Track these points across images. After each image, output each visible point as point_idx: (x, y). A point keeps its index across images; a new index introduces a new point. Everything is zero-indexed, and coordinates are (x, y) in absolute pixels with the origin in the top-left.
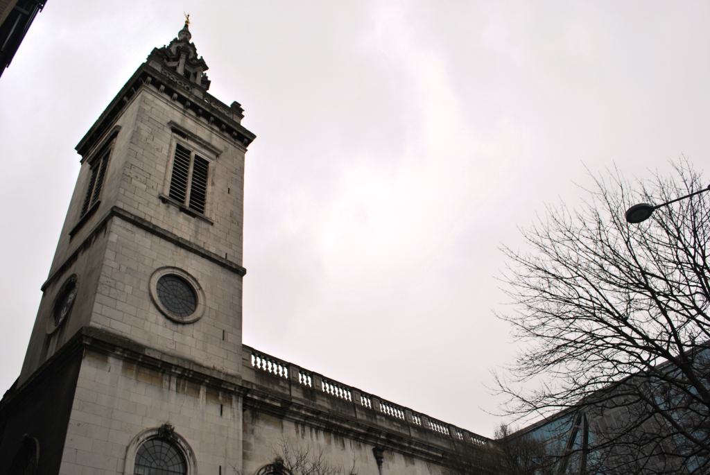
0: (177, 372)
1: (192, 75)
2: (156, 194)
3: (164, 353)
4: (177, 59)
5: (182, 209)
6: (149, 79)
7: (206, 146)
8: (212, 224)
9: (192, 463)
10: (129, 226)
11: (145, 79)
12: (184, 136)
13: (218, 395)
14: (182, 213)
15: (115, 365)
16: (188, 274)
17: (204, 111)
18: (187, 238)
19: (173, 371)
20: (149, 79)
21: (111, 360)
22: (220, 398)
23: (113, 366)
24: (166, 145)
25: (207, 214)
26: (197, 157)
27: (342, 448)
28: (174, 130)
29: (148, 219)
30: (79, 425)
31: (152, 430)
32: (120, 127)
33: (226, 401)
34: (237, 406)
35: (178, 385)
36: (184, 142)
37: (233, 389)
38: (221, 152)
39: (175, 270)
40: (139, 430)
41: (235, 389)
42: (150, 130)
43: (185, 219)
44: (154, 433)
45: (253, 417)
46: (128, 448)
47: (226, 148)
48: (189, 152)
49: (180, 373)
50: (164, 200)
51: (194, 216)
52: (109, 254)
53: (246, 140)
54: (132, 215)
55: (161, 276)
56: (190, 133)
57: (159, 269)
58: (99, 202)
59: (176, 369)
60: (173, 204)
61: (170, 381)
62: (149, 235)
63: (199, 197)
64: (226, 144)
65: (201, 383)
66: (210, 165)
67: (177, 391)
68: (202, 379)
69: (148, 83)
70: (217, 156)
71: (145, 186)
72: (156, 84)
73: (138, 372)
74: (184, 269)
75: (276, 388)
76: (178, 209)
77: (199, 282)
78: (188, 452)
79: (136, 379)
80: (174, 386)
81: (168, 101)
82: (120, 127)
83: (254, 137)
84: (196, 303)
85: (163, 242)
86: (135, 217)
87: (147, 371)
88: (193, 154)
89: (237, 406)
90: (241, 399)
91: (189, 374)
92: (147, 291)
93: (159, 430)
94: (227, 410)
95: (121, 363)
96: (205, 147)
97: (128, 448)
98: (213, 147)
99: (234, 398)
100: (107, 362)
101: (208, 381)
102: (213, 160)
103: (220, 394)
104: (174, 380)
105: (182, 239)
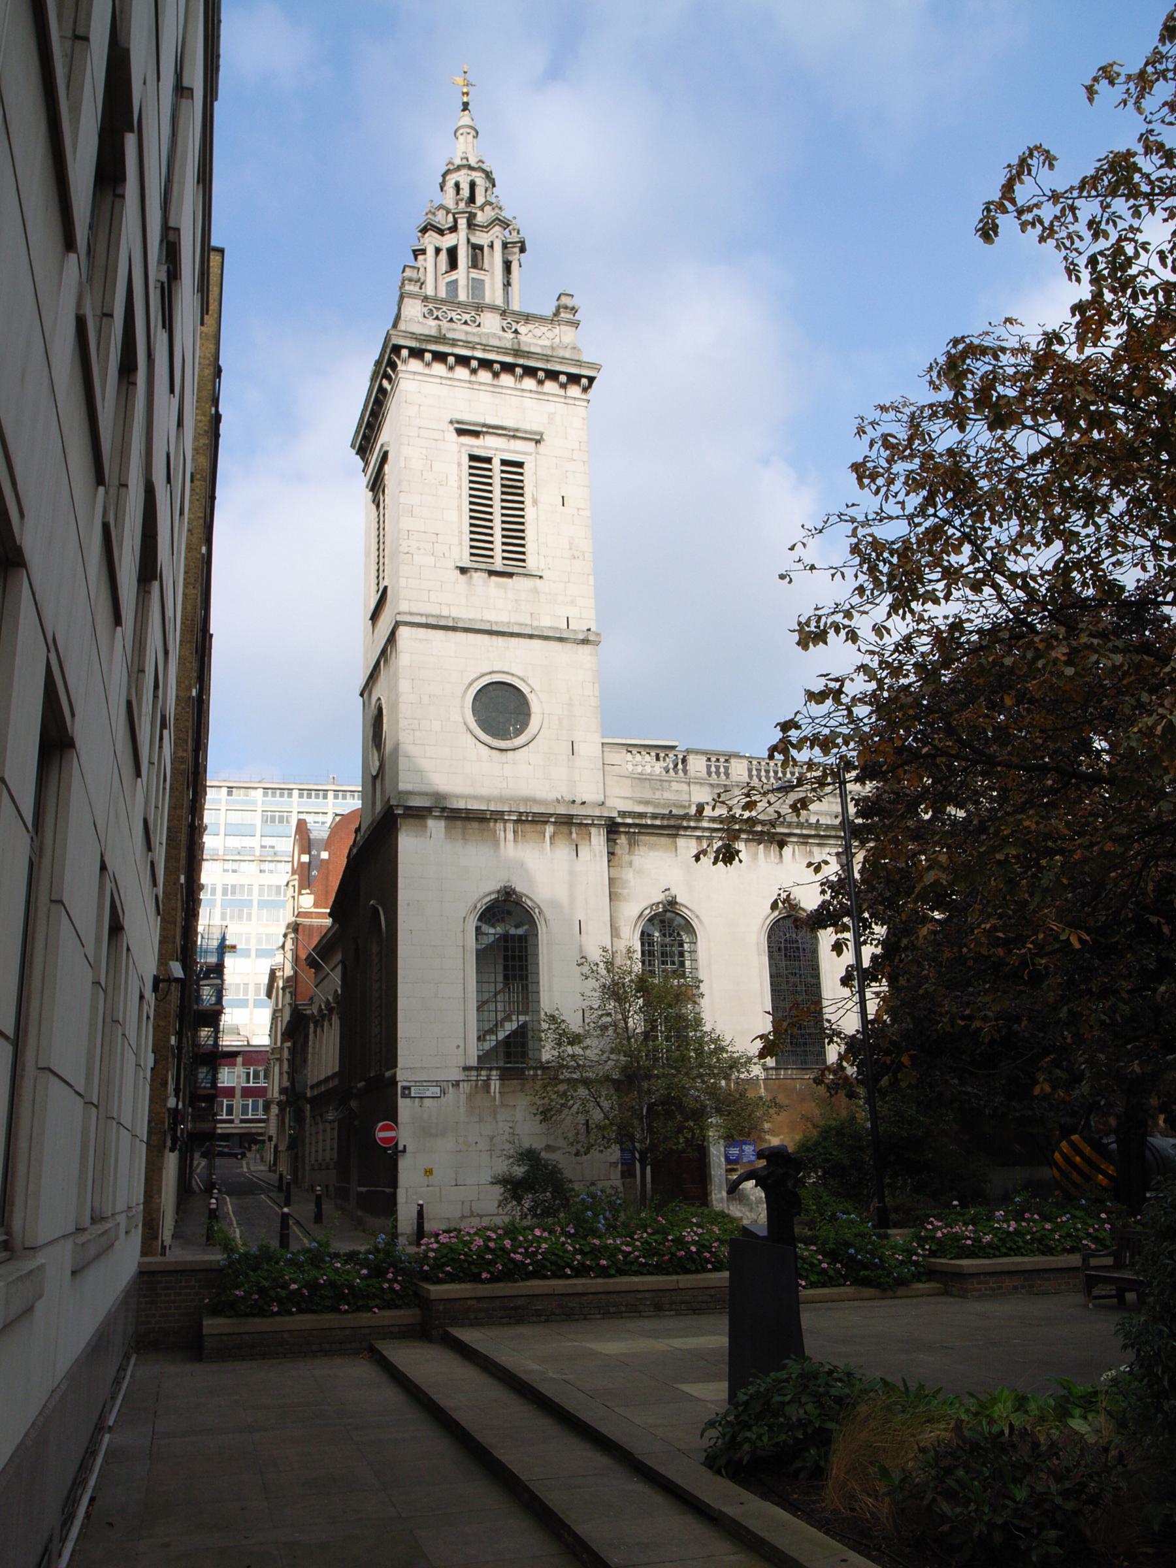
0: (512, 818)
1: (486, 249)
2: (452, 565)
3: (489, 800)
4: (454, 229)
5: (492, 573)
6: (405, 353)
7: (513, 434)
8: (541, 577)
9: (543, 922)
10: (422, 632)
11: (399, 356)
12: (476, 434)
13: (571, 833)
14: (494, 579)
15: (436, 826)
16: (513, 675)
17: (502, 364)
18: (504, 618)
19: (506, 817)
20: (405, 353)
21: (430, 823)
22: (574, 835)
23: (434, 830)
24: (458, 449)
25: (532, 563)
26: (504, 462)
27: (777, 861)
28: (461, 432)
29: (445, 613)
30: (408, 905)
31: (490, 894)
32: (388, 443)
33: (583, 839)
34: (599, 842)
35: (514, 832)
36: (477, 447)
37: (590, 822)
38: (541, 434)
39: (493, 676)
40: (476, 897)
41: (593, 820)
42: (424, 451)
43: (498, 586)
44: (493, 897)
45: (630, 844)
46: (465, 918)
47: (551, 417)
48: (488, 460)
49: (515, 818)
50: (463, 570)
51: (510, 575)
52: (404, 686)
53: (584, 381)
54: (421, 615)
55: (475, 692)
56: (484, 425)
57: (471, 684)
58: (386, 588)
59: (509, 815)
60: (476, 570)
61: (505, 831)
62: (450, 634)
63: (515, 534)
64: (550, 407)
65: (546, 822)
66: (525, 466)
67: (515, 841)
68: (546, 819)
69: (404, 361)
70: (538, 442)
71: (433, 558)
72: (416, 353)
73: (464, 829)
74: (505, 669)
75: (667, 795)
76: (487, 575)
77: (529, 682)
78: (537, 910)
79: (464, 838)
80: (510, 835)
81: (441, 377)
82: (388, 443)
83: (597, 367)
84: (528, 715)
85: (471, 637)
86: (427, 616)
87: (475, 825)
88: (496, 463)
89: (598, 839)
90: (603, 832)
91: (527, 816)
92: (461, 720)
93: (498, 892)
94: (584, 851)
95: (442, 824)
96: (514, 437)
97: (465, 918)
98: (526, 432)
99: (593, 830)
100: (426, 827)
101: (553, 820)
102: (530, 454)
103: (574, 830)
104: (510, 826)
105: (496, 623)
